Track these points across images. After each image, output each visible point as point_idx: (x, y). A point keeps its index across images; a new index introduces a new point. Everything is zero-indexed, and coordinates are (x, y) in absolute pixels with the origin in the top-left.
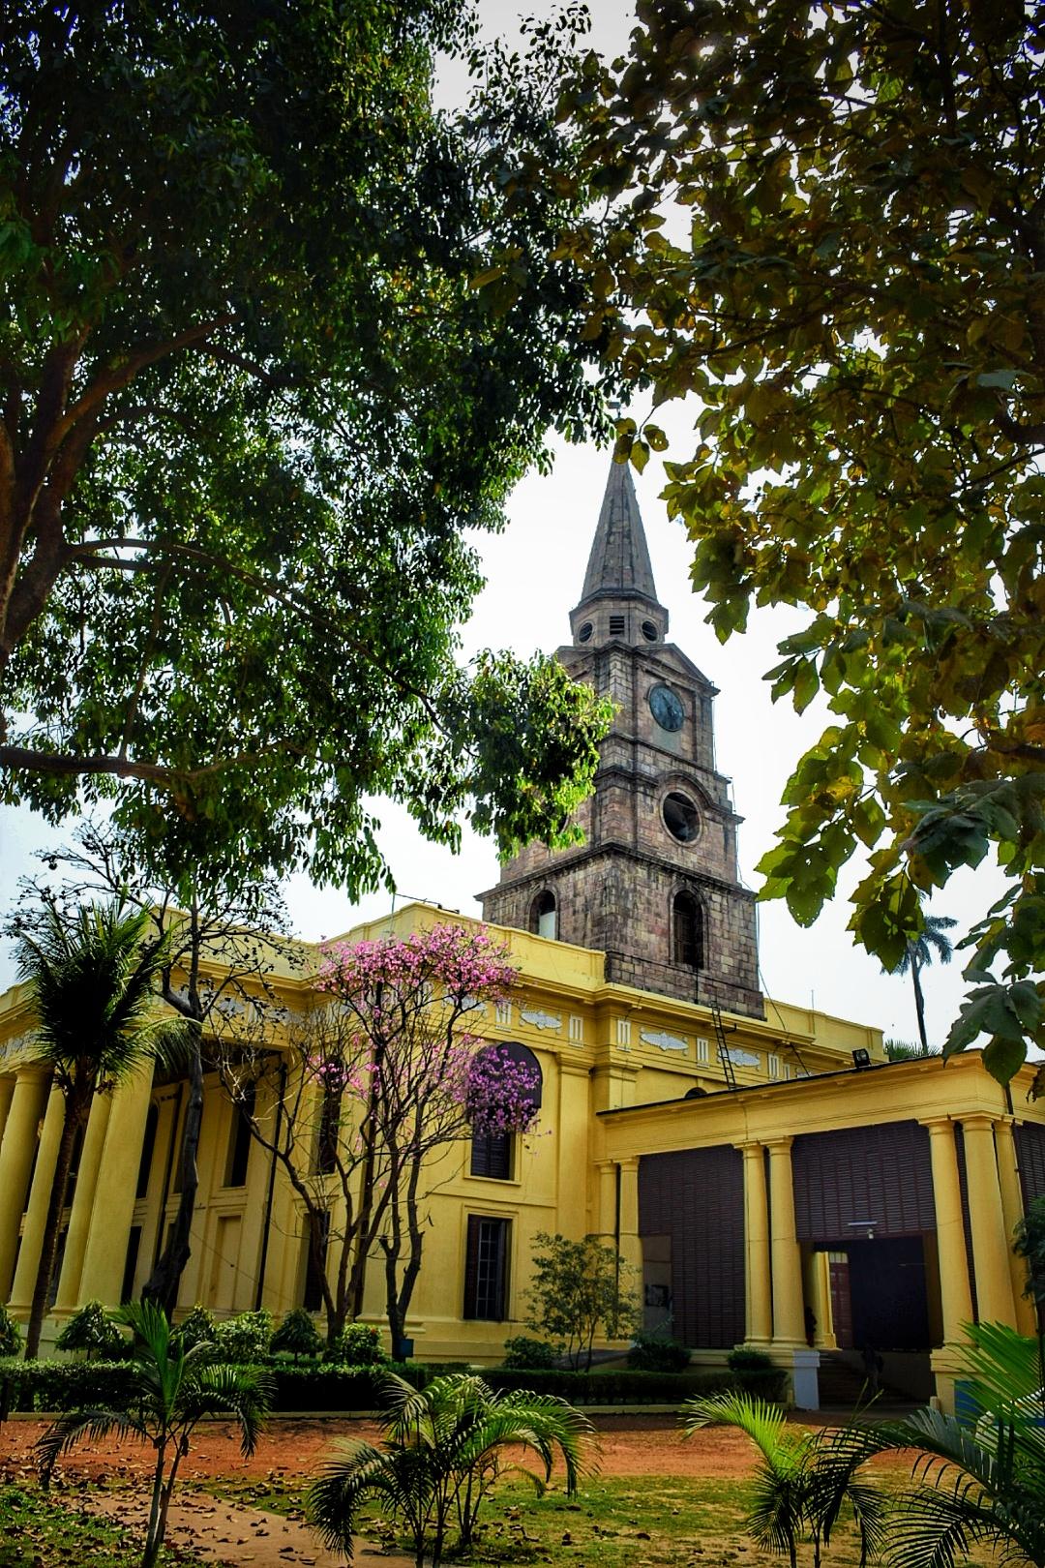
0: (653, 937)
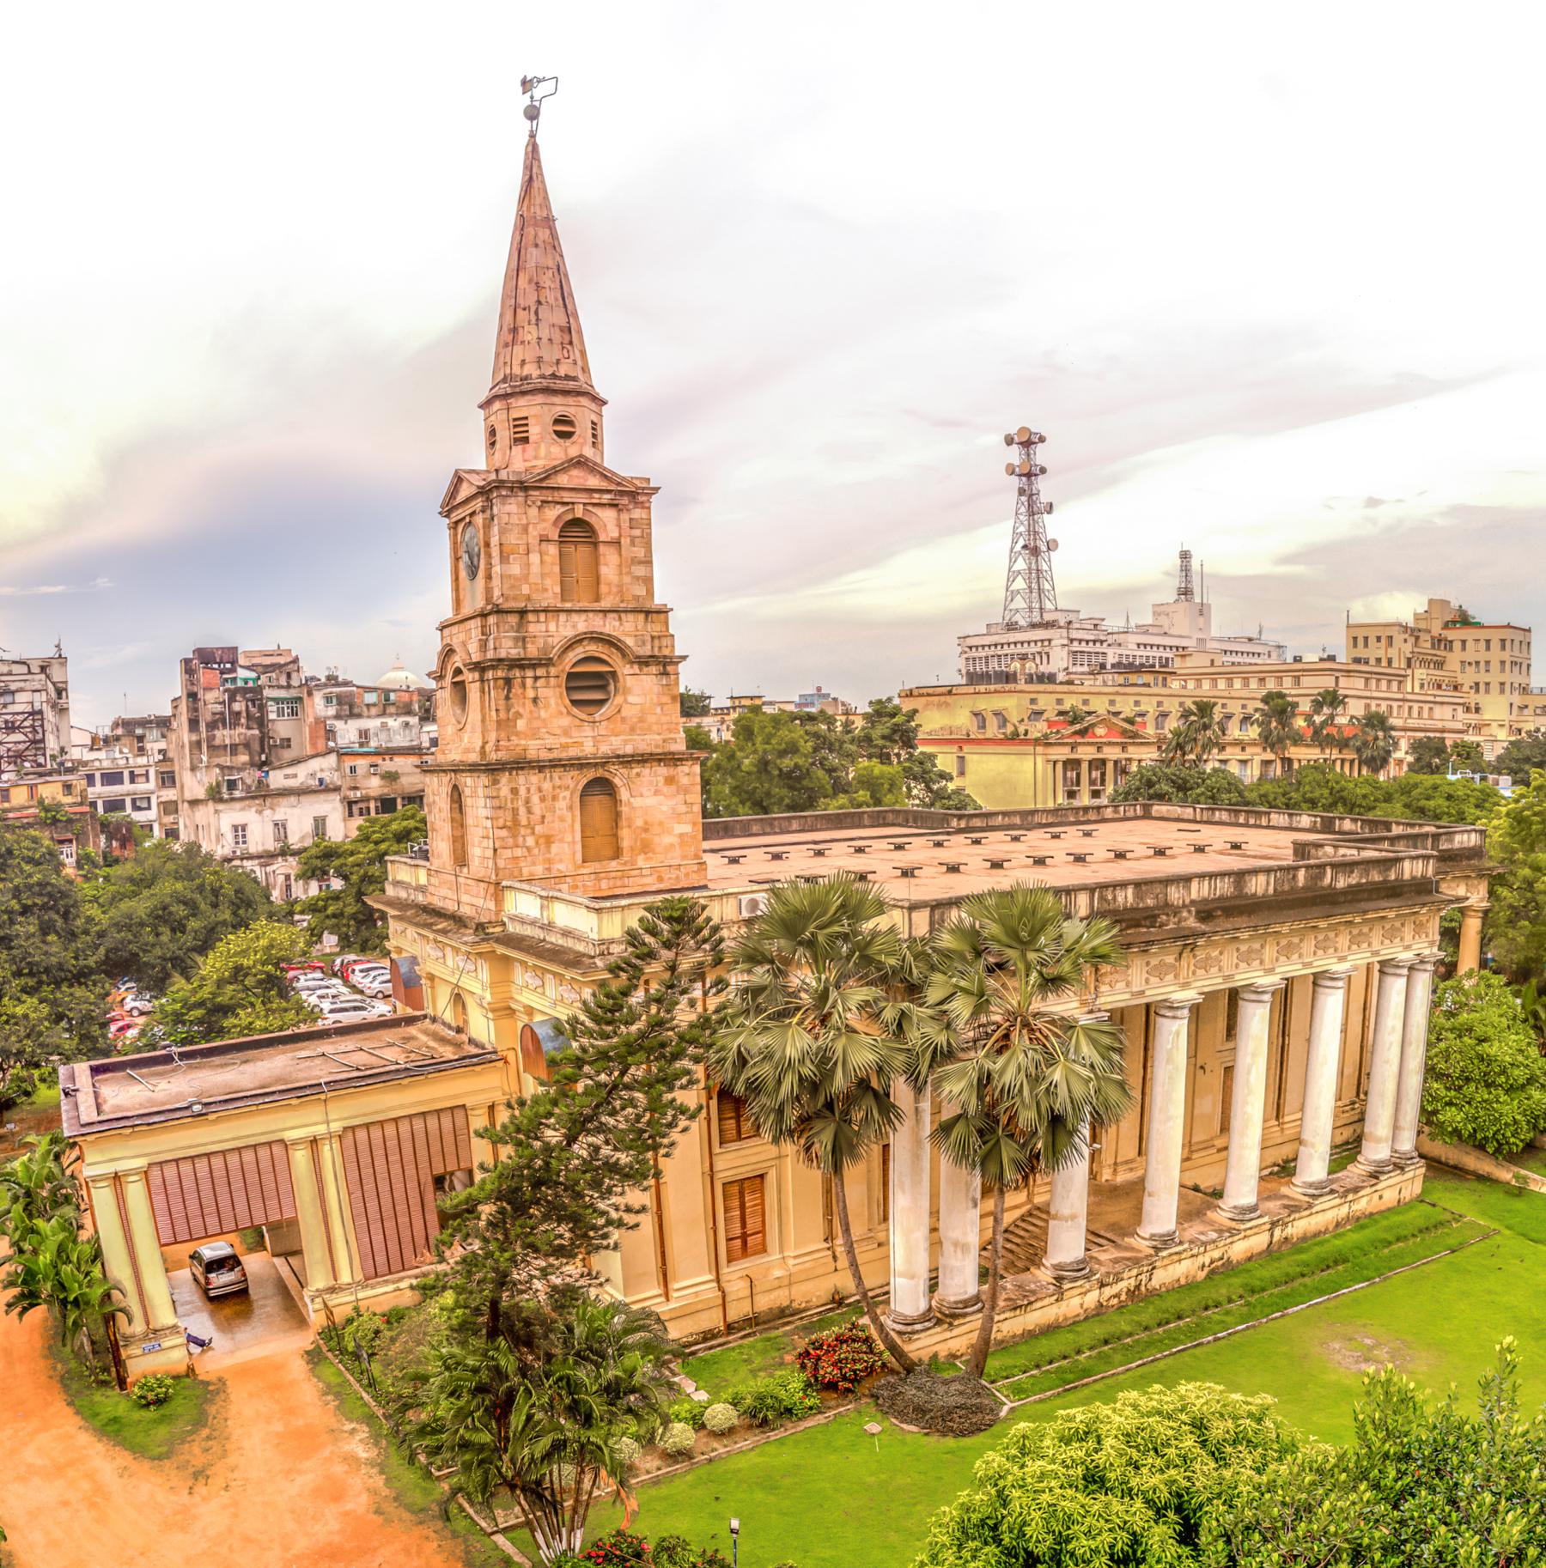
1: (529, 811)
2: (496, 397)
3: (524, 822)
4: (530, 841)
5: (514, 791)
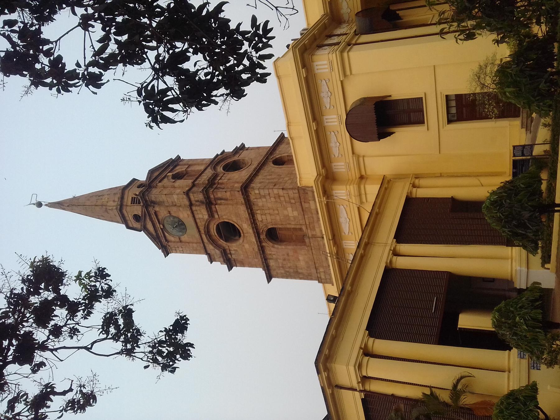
0: (301, 258)
1: (273, 179)
2: (121, 210)
3: (277, 180)
4: (287, 179)
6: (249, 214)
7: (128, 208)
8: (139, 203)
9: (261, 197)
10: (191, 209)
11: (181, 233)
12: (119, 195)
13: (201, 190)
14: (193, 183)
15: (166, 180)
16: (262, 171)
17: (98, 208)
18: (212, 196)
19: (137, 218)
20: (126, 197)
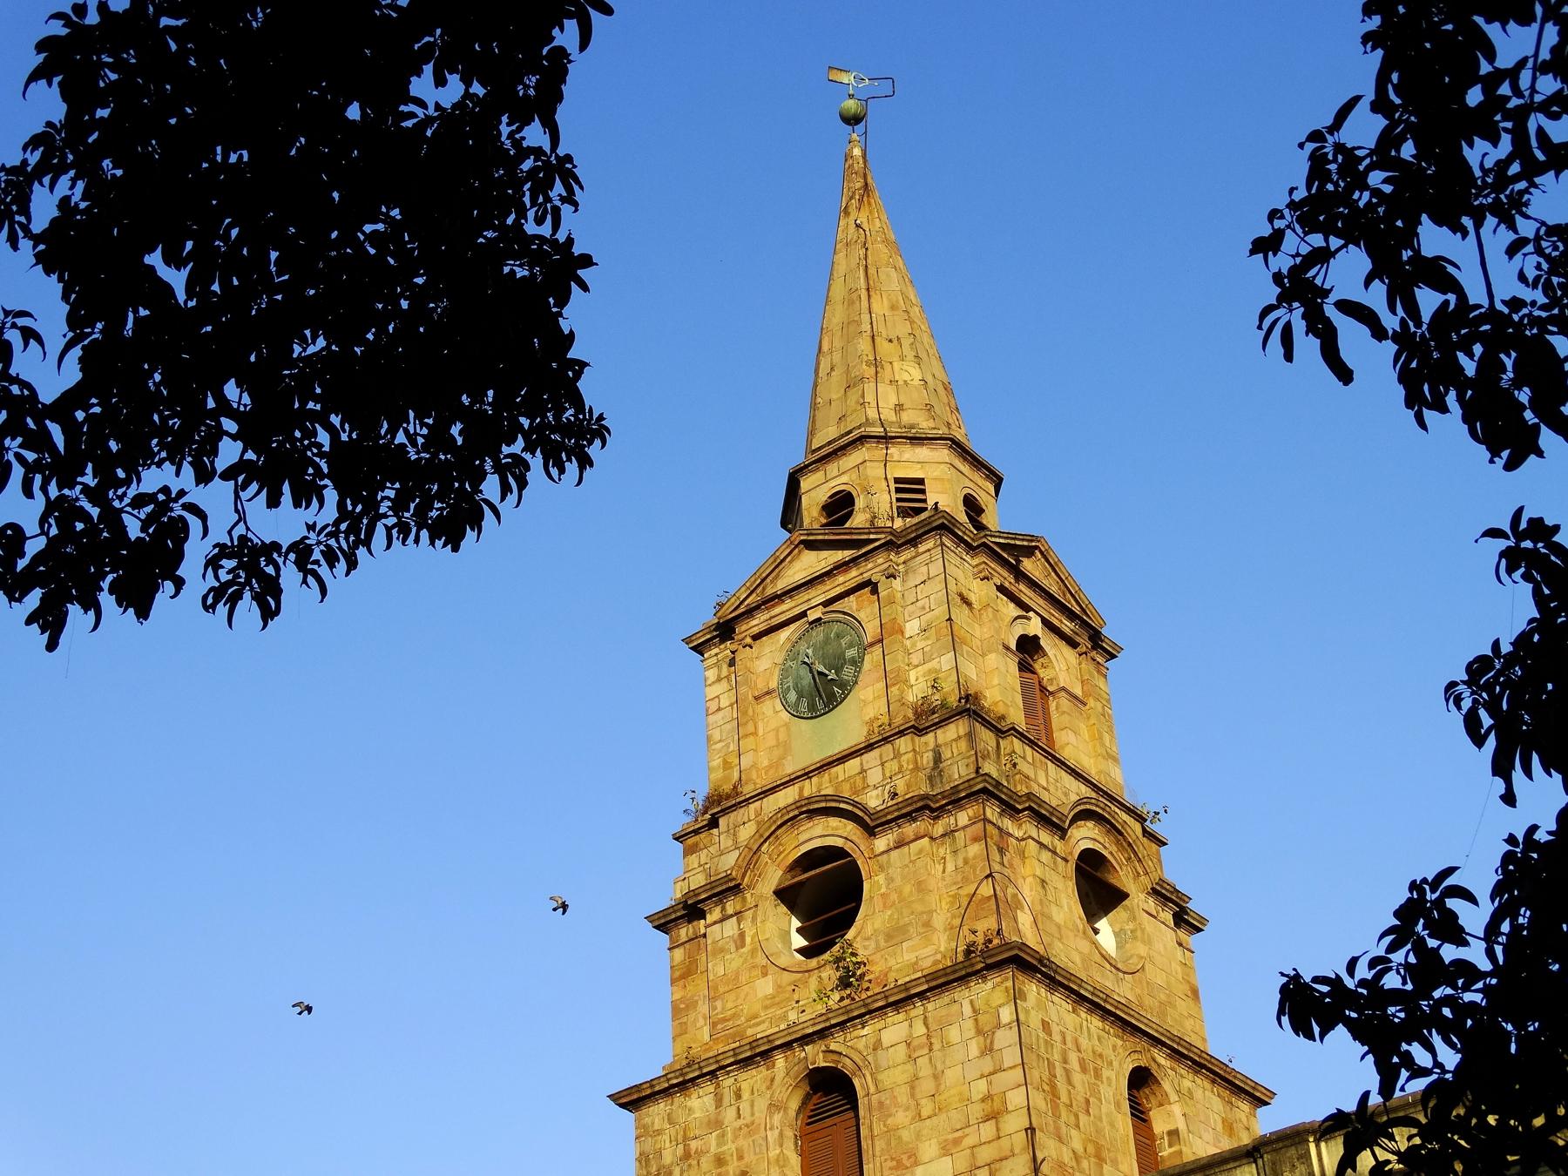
1: (1069, 1082)
3: (1064, 1098)
4: (1077, 1145)
5: (1046, 1026)
6: (906, 986)
7: (875, 471)
8: (904, 513)
9: (986, 1034)
10: (901, 733)
11: (792, 696)
12: (925, 425)
13: (989, 768)
14: (1014, 730)
15: (1012, 610)
16: (1096, 1022)
17: (864, 345)
18: (963, 818)
19: (840, 505)
20: (923, 452)
